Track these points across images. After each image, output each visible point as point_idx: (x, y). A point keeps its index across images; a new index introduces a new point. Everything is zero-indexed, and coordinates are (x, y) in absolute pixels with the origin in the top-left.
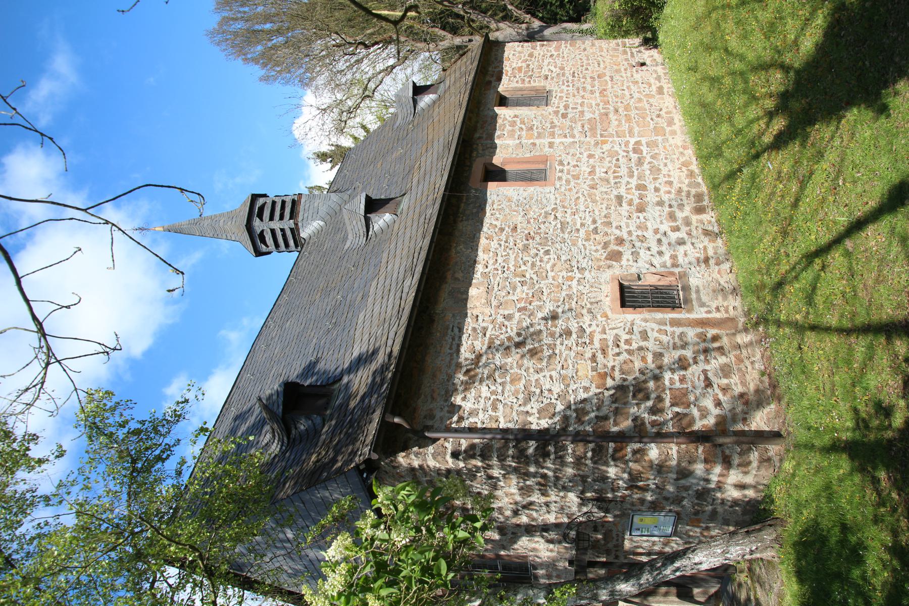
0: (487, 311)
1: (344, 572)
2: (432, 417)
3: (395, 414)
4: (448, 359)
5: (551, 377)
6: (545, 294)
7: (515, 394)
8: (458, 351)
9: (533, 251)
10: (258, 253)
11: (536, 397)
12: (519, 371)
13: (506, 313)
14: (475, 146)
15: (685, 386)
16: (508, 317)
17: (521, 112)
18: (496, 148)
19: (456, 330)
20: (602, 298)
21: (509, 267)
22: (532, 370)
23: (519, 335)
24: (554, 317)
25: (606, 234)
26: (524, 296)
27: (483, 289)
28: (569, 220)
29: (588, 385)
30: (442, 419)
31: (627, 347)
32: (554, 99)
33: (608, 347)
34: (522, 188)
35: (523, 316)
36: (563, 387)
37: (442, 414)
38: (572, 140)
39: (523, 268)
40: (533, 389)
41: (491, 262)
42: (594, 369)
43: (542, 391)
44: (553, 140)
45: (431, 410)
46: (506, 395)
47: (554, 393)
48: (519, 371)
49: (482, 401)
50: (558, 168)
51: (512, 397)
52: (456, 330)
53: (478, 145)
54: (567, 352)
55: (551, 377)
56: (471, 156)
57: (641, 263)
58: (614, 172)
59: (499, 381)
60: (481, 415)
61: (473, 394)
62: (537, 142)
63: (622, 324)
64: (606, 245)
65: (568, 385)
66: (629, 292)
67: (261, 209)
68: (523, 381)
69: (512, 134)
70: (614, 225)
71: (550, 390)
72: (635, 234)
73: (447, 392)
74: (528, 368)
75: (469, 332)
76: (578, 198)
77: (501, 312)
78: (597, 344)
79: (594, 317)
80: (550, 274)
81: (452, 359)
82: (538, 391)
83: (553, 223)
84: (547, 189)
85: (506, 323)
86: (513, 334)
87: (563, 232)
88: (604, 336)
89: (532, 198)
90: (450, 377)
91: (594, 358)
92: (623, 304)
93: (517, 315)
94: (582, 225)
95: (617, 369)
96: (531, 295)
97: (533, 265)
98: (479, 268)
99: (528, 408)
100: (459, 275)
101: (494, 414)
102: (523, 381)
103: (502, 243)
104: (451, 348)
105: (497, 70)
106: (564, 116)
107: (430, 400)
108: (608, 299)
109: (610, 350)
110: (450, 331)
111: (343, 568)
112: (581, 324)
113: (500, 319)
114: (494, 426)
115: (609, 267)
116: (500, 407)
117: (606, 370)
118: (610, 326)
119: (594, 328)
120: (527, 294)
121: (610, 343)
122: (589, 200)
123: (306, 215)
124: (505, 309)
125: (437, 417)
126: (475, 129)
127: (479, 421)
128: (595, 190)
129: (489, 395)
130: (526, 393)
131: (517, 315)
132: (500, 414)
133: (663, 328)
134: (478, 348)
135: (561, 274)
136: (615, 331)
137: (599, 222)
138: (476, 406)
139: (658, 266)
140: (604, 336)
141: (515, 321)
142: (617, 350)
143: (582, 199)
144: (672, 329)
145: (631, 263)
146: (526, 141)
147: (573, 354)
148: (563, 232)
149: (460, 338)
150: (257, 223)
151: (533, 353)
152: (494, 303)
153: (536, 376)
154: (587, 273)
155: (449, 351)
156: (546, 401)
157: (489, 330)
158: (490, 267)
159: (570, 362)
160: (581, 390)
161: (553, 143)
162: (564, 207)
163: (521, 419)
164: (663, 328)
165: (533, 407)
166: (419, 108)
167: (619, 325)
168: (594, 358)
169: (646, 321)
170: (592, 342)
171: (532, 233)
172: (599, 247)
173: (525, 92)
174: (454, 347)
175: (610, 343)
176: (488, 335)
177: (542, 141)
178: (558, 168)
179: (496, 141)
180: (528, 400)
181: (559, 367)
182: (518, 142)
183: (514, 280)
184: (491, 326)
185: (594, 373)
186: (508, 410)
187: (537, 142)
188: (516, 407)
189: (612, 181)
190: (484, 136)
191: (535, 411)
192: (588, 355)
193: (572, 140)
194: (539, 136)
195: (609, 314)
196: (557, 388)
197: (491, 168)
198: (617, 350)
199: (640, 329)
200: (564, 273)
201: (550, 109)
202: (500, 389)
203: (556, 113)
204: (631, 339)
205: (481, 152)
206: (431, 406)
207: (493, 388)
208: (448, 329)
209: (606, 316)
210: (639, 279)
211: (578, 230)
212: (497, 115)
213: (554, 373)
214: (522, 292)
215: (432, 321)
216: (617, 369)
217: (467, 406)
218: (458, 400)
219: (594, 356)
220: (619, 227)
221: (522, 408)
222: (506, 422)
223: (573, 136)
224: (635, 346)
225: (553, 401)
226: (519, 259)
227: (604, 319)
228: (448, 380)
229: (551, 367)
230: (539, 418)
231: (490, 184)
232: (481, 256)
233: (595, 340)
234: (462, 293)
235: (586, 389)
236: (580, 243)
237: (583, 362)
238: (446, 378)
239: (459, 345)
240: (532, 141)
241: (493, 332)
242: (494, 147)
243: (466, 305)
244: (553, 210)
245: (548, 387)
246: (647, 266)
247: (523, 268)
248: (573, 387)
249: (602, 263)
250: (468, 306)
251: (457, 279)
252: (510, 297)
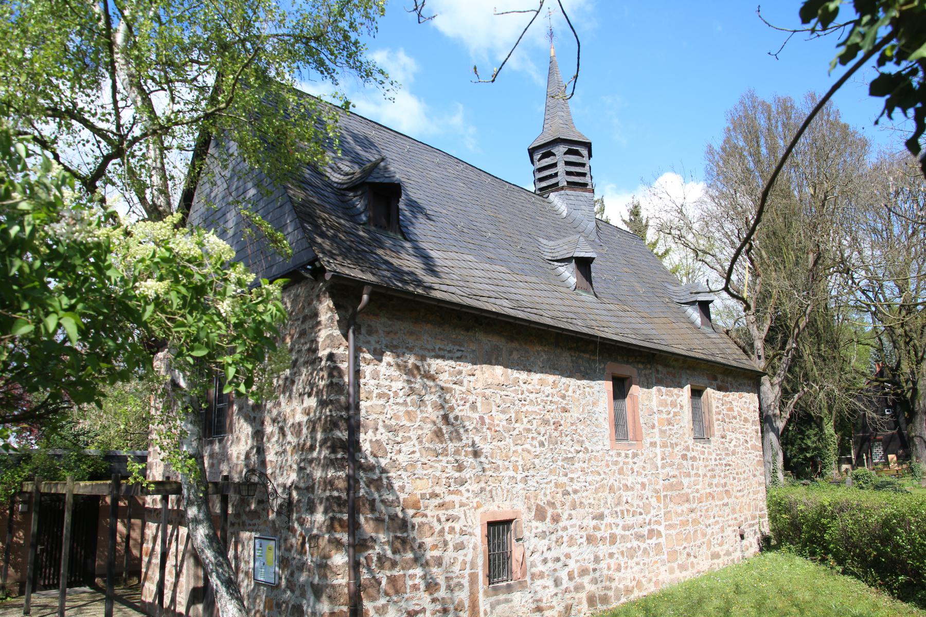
0: (479, 385)
1: (192, 253)
2: (370, 332)
3: (371, 296)
4: (429, 347)
5: (413, 452)
6: (499, 443)
7: (395, 417)
8: (437, 357)
9: (542, 430)
10: (532, 152)
11: (392, 437)
12: (418, 419)
13: (478, 404)
14: (649, 366)
15: (408, 591)
16: (473, 407)
17: (686, 412)
18: (648, 388)
19: (459, 354)
20: (496, 502)
21: (525, 405)
22: (420, 432)
23: (456, 418)
24: (476, 454)
25: (563, 504)
26: (496, 422)
27: (502, 380)
28: (576, 465)
29: (406, 490)
30: (368, 342)
31: (447, 529)
33: (447, 509)
34: (607, 416)
35: (475, 422)
36: (404, 464)
37: (373, 343)
38: (660, 466)
39: (525, 420)
40: (401, 434)
41: (530, 387)
42: (423, 496)
43: (399, 443)
44: (658, 446)
45: (377, 331)
46: (394, 407)
47: (397, 456)
48: (418, 419)
49: (387, 383)
50: (630, 452)
51: (392, 413)
52: (459, 354)
54: (440, 468)
55: (413, 452)
56: (638, 362)
57: (534, 541)
58: (628, 511)
59: (409, 399)
60: (372, 382)
61: (394, 373)
62: (656, 430)
63: (470, 523)
64: (552, 504)
65: (406, 470)
66: (503, 530)
67: (577, 153)
68: (408, 424)
69: (663, 403)
70: (573, 512)
71: (400, 451)
72: (564, 534)
73: (396, 347)
74: (422, 429)
75: (458, 368)
76: (600, 474)
77: (479, 399)
78: (448, 498)
79: (476, 495)
80: (519, 448)
81: (429, 350)
82: (399, 439)
83: (572, 450)
84: (607, 442)
85: (468, 405)
86: (457, 412)
87: (563, 460)
88: (457, 506)
89: (597, 426)
90: (410, 350)
91: (435, 495)
92: (490, 524)
93: (476, 416)
94: (572, 479)
95: (424, 520)
96: (497, 429)
97: (528, 430)
98: (523, 375)
99: (381, 430)
100: (515, 355)
101: (374, 395)
102: (408, 424)
103: (550, 398)
104: (440, 349)
105: (729, 385)
106: (684, 457)
107: (386, 330)
108: (496, 508)
109: (444, 512)
110: (458, 348)
111: (196, 252)
112: (469, 482)
113: (471, 398)
114: (362, 396)
115: (529, 508)
116: (382, 401)
117: (422, 508)
118: (467, 512)
119: (466, 494)
120: (498, 425)
121: (450, 512)
123: (572, 198)
124: (482, 403)
125: (369, 338)
126: (666, 366)
127: (368, 382)
129: (394, 389)
130: (397, 427)
131: (476, 416)
132: (375, 401)
133: (468, 566)
134: (441, 376)
135: (520, 459)
136: (463, 517)
137: (575, 497)
138: (382, 377)
139: (532, 559)
140: (457, 506)
141: (470, 414)
142: (443, 519)
143: (598, 478)
144: (466, 575)
145: (534, 531)
147: (438, 474)
148: (563, 460)
149: (451, 358)
150: (562, 149)
151: (438, 434)
152: (488, 392)
153: (414, 437)
154: (521, 485)
155: (437, 348)
156: (388, 447)
157: (461, 388)
158: (525, 387)
159: (430, 471)
160: (401, 484)
162: (590, 460)
163: (370, 423)
164: (468, 566)
165: (383, 435)
166: (686, 307)
167: (469, 520)
168: (435, 495)
169: (475, 548)
170: (450, 493)
171: (561, 428)
172: (549, 498)
174: (441, 353)
175: (450, 512)
176: (454, 386)
177: (657, 435)
178: (630, 452)
179: (655, 388)
180: (390, 429)
181: (424, 460)
182: (655, 410)
183: (512, 411)
184: (464, 389)
185: (419, 496)
186: (379, 410)
187: (656, 430)
188: (382, 417)
189: (618, 509)
190: (660, 376)
191: (378, 437)
192: (438, 490)
193: (660, 466)
194: (662, 432)
195: (481, 510)
196: (402, 459)
197: (627, 383)
198: (443, 519)
199: (465, 542)
200: (521, 462)
201: (691, 442)
202: (401, 401)
203: (687, 449)
204: (455, 533)
205: (643, 372)
206: (380, 331)
207: (401, 393)
208: (460, 345)
209: (478, 507)
210: (518, 540)
211: (566, 475)
212: (682, 387)
213: (417, 455)
214: (500, 419)
215: (467, 329)
216: (424, 520)
217: (382, 368)
218: (388, 358)
219: (437, 495)
220: (570, 517)
221: (381, 423)
222: (366, 407)
223: (663, 467)
224: (448, 537)
225: (389, 455)
226: (534, 416)
227: (475, 505)
228: (407, 348)
229: (424, 452)
230: (371, 441)
231: (611, 383)
232: (536, 377)
233: (453, 496)
234: (497, 359)
235: (402, 488)
236: (552, 477)
237: (431, 484)
238: (410, 345)
239: (443, 357)
240: (657, 424)
241: (458, 392)
242: (649, 386)
243: (485, 363)
244: (586, 449)
245: (404, 449)
246: (531, 548)
247: (525, 420)
248: (404, 475)
249: (533, 501)
250: (484, 366)
251: (511, 353)
252: (494, 408)
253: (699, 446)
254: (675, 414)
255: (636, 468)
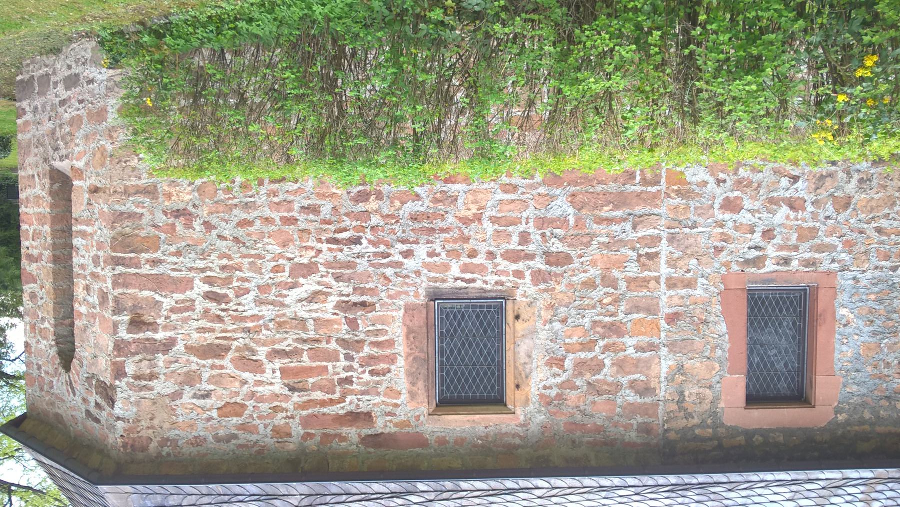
14: (672, 435)
32: (479, 284)
50: (770, 266)
53: (666, 431)
58: (795, 163)
76: (879, 230)
84: (844, 280)
89: (872, 311)
105: (297, 430)
106: (551, 258)
122: (887, 211)
128: (854, 201)
143: (884, 223)
146: (663, 334)
161: (669, 279)
173: (431, 349)
178: (770, 266)
182: (664, 351)
194: (651, 309)
203: (539, 277)
205: (696, 421)
223: (655, 240)
240: (663, 323)
253: (486, 282)
254: (588, 346)
255: (757, 238)
